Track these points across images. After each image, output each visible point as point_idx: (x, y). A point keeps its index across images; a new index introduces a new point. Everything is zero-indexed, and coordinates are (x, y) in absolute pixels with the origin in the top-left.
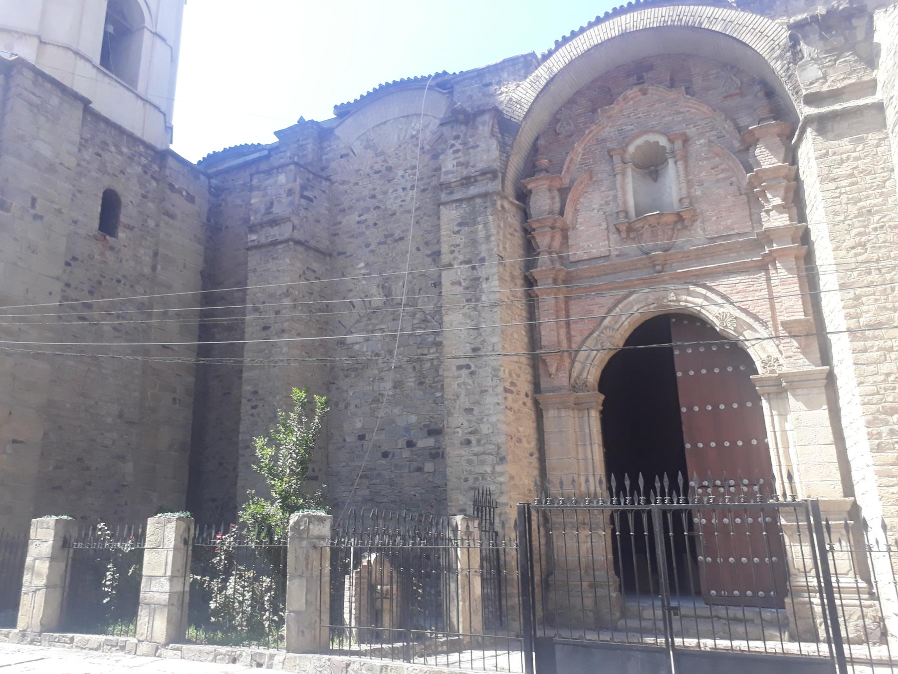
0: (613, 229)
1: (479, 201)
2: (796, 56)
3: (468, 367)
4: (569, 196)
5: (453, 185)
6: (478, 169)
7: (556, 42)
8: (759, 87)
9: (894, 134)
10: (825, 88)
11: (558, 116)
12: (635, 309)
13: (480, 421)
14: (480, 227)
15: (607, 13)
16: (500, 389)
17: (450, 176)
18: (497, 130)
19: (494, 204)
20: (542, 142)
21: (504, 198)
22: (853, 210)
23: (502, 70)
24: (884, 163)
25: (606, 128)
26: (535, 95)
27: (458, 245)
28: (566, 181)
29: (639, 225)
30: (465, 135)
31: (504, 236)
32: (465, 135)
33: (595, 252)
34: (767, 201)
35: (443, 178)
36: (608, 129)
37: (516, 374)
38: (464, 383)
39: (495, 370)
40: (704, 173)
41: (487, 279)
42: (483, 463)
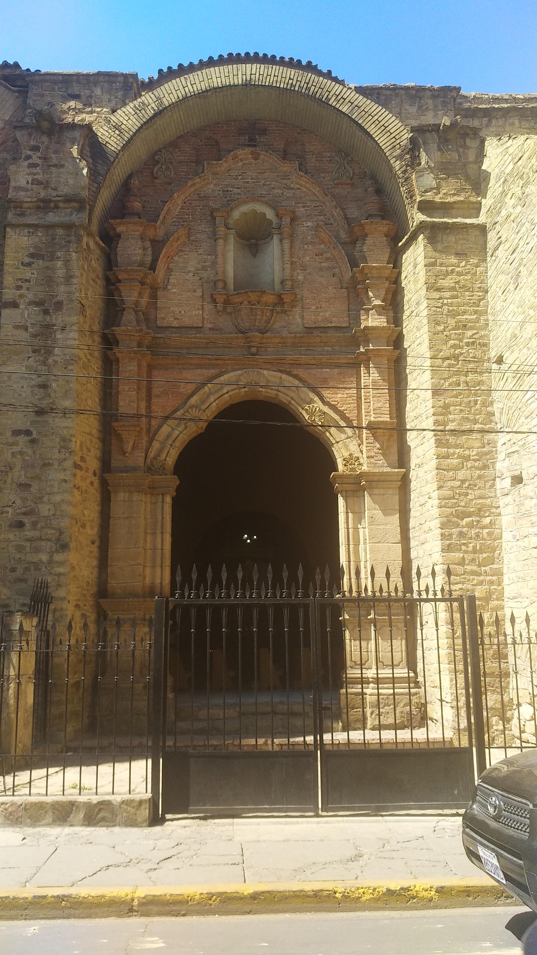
0: (208, 298)
1: (60, 232)
2: (414, 162)
3: (28, 433)
4: (163, 252)
7: (160, 71)
8: (370, 182)
9: (494, 258)
10: (437, 199)
11: (156, 158)
12: (225, 391)
13: (39, 499)
14: (59, 264)
15: (221, 56)
16: (69, 464)
17: (22, 193)
18: (89, 154)
19: (79, 240)
20: (135, 182)
21: (90, 234)
22: (452, 322)
23: (96, 84)
24: (481, 283)
25: (210, 184)
26: (139, 125)
28: (161, 233)
29: (237, 300)
30: (47, 148)
32: (47, 148)
33: (187, 322)
34: (369, 299)
35: (11, 194)
36: (212, 186)
38: (21, 453)
39: (64, 439)
40: (308, 258)
41: (63, 329)
42: (37, 550)
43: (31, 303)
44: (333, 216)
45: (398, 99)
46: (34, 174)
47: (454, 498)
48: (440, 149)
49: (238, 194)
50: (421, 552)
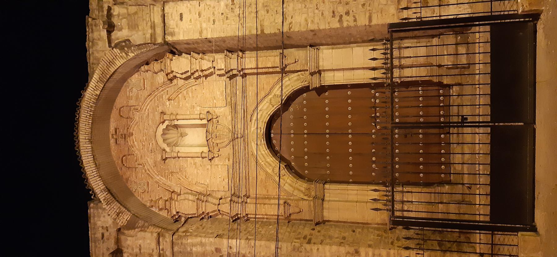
1: (176, 249)
6: (155, 248)
16: (308, 247)
26: (116, 202)
31: (204, 233)
36: (149, 159)
37: (298, 235)
40: (187, 105)
41: (231, 248)
44: (163, 91)
47: (325, 18)
48: (121, 30)
50: (358, 36)
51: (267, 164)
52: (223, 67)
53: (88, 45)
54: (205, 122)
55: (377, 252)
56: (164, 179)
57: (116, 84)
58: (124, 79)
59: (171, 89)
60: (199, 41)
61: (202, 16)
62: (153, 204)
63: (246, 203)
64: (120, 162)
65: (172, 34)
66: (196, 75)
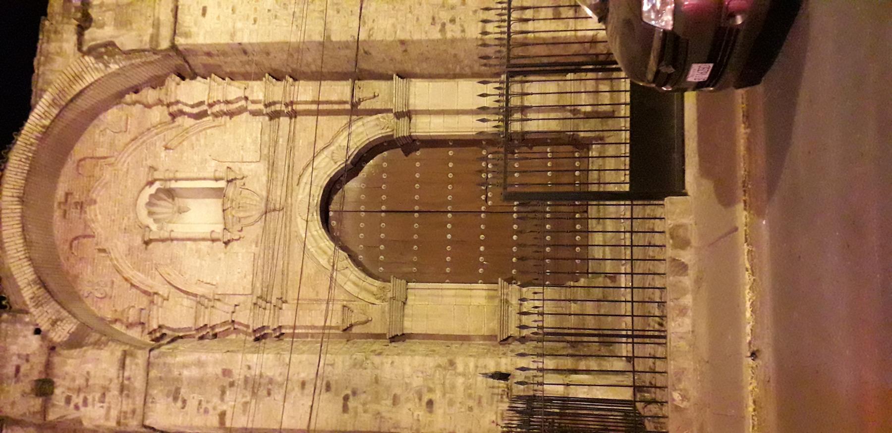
1: (153, 373)
3: (346, 398)
5: (125, 408)
14: (186, 373)
16: (377, 360)
26: (53, 303)
27: (200, 403)
35: (112, 424)
36: (119, 243)
38: (364, 404)
39: (355, 365)
40: (196, 157)
41: (249, 368)
43: (222, 399)
45: (48, 73)
46: (94, 400)
48: (102, 26)
49: (129, 218)
51: (319, 251)
52: (261, 97)
53: (39, 60)
54: (222, 184)
55: (481, 362)
56: (142, 276)
57: (79, 116)
58: (94, 113)
59: (170, 134)
60: (227, 49)
61: (237, 12)
62: (117, 316)
63: (281, 309)
64: (66, 247)
65: (187, 35)
66: (216, 108)
